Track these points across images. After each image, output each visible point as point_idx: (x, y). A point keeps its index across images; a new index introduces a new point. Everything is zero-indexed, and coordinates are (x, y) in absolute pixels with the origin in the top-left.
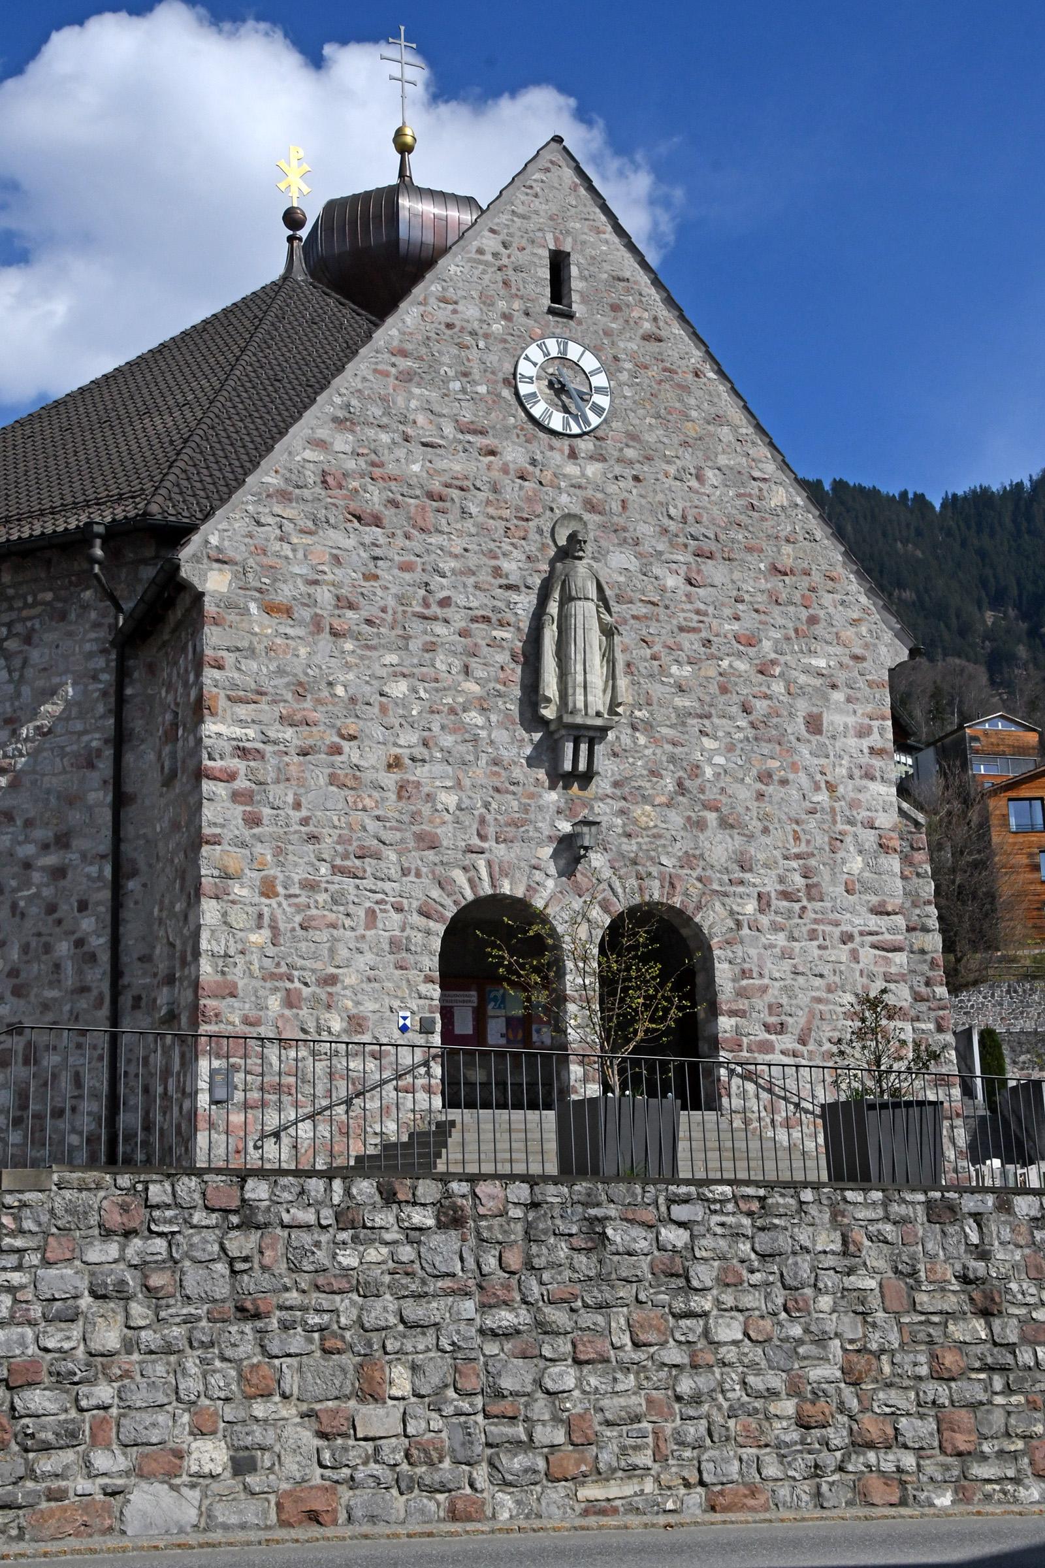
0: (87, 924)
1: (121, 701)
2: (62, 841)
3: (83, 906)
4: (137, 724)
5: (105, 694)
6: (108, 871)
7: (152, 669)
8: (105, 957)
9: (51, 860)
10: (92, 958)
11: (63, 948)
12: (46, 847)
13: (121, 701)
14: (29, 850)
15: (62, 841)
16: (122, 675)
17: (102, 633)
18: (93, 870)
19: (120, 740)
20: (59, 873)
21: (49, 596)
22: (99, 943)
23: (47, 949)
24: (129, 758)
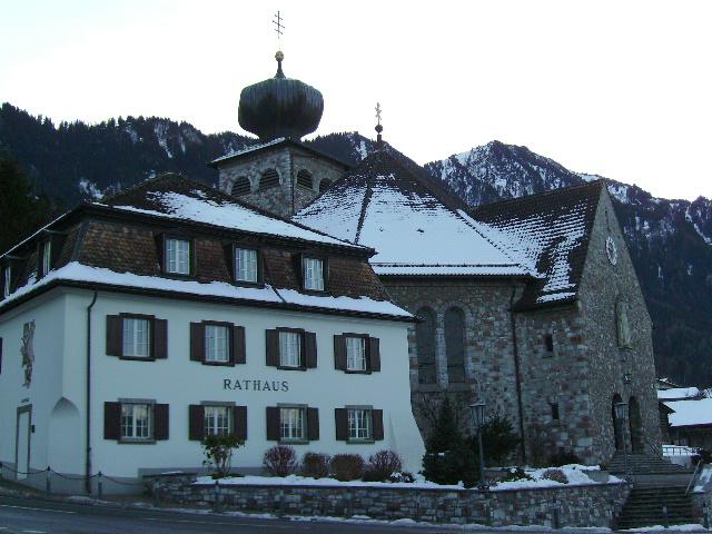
0: (508, 395)
1: (514, 328)
2: (496, 369)
3: (506, 389)
4: (518, 336)
5: (506, 326)
6: (514, 379)
7: (522, 320)
8: (516, 404)
9: (493, 374)
10: (510, 405)
11: (500, 402)
12: (491, 370)
13: (514, 328)
14: (486, 370)
15: (496, 369)
16: (513, 321)
17: (503, 306)
18: (509, 379)
19: (514, 339)
20: (496, 379)
21: (483, 292)
22: (513, 400)
23: (495, 401)
24: (518, 346)
